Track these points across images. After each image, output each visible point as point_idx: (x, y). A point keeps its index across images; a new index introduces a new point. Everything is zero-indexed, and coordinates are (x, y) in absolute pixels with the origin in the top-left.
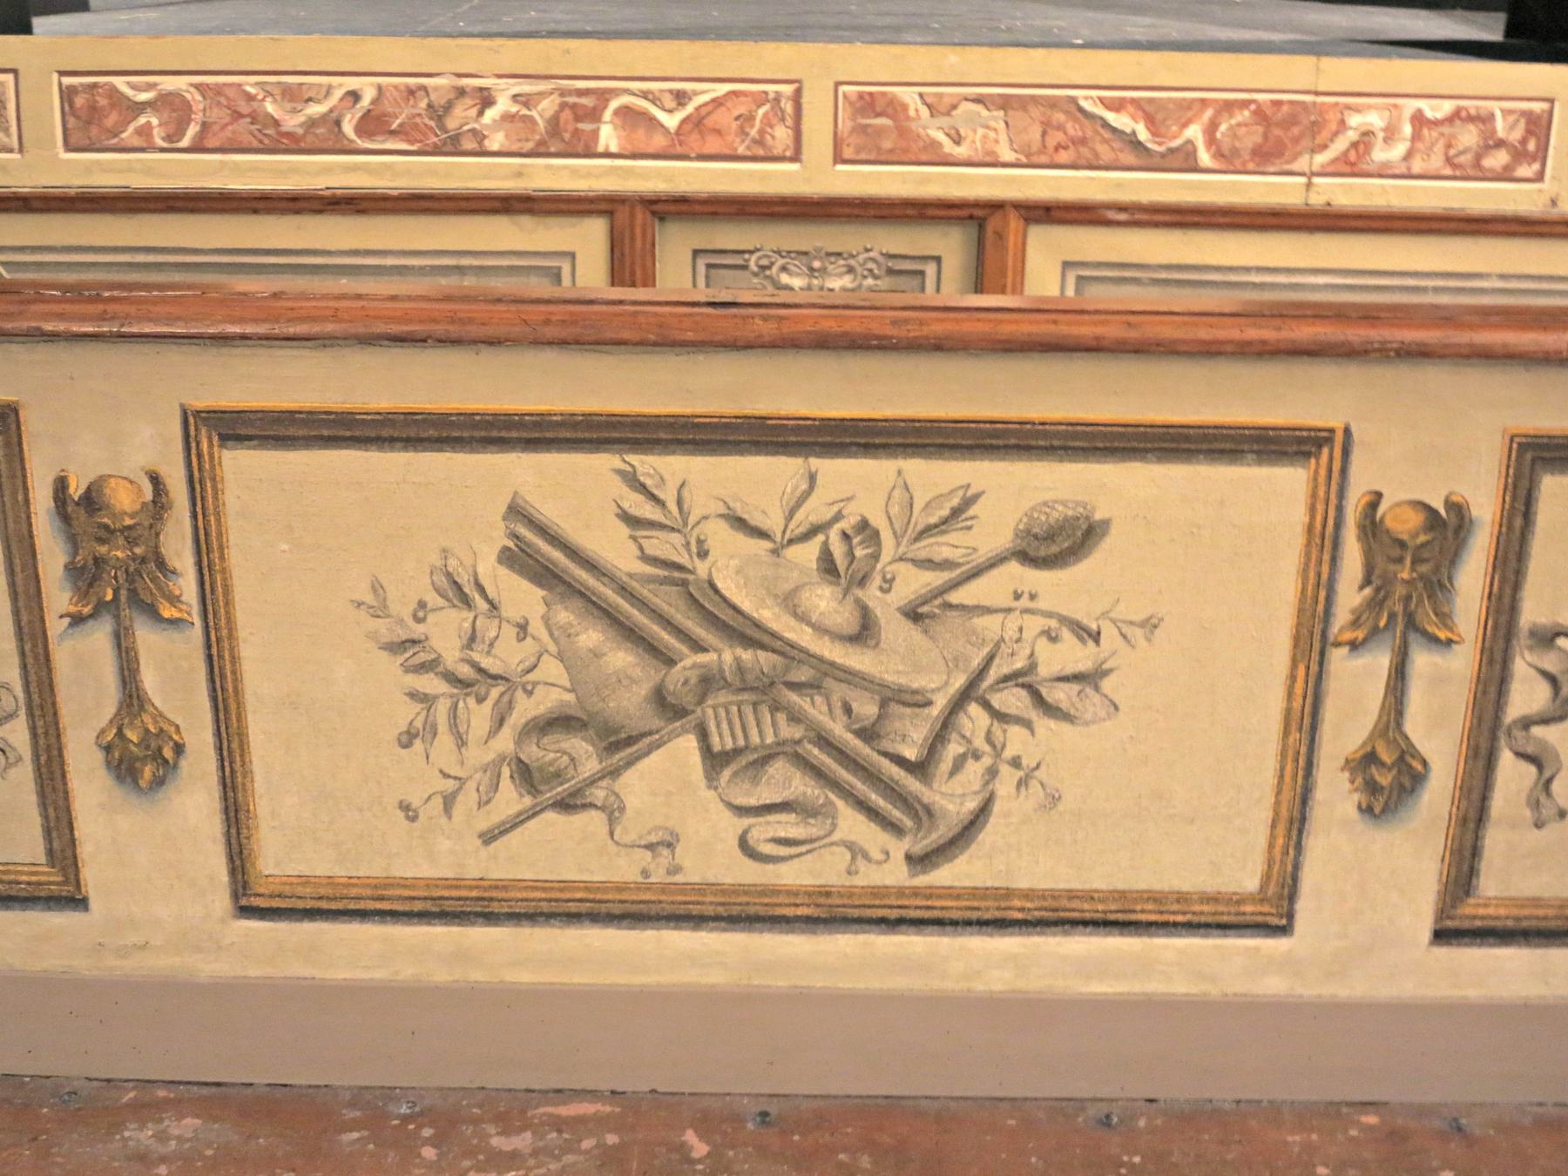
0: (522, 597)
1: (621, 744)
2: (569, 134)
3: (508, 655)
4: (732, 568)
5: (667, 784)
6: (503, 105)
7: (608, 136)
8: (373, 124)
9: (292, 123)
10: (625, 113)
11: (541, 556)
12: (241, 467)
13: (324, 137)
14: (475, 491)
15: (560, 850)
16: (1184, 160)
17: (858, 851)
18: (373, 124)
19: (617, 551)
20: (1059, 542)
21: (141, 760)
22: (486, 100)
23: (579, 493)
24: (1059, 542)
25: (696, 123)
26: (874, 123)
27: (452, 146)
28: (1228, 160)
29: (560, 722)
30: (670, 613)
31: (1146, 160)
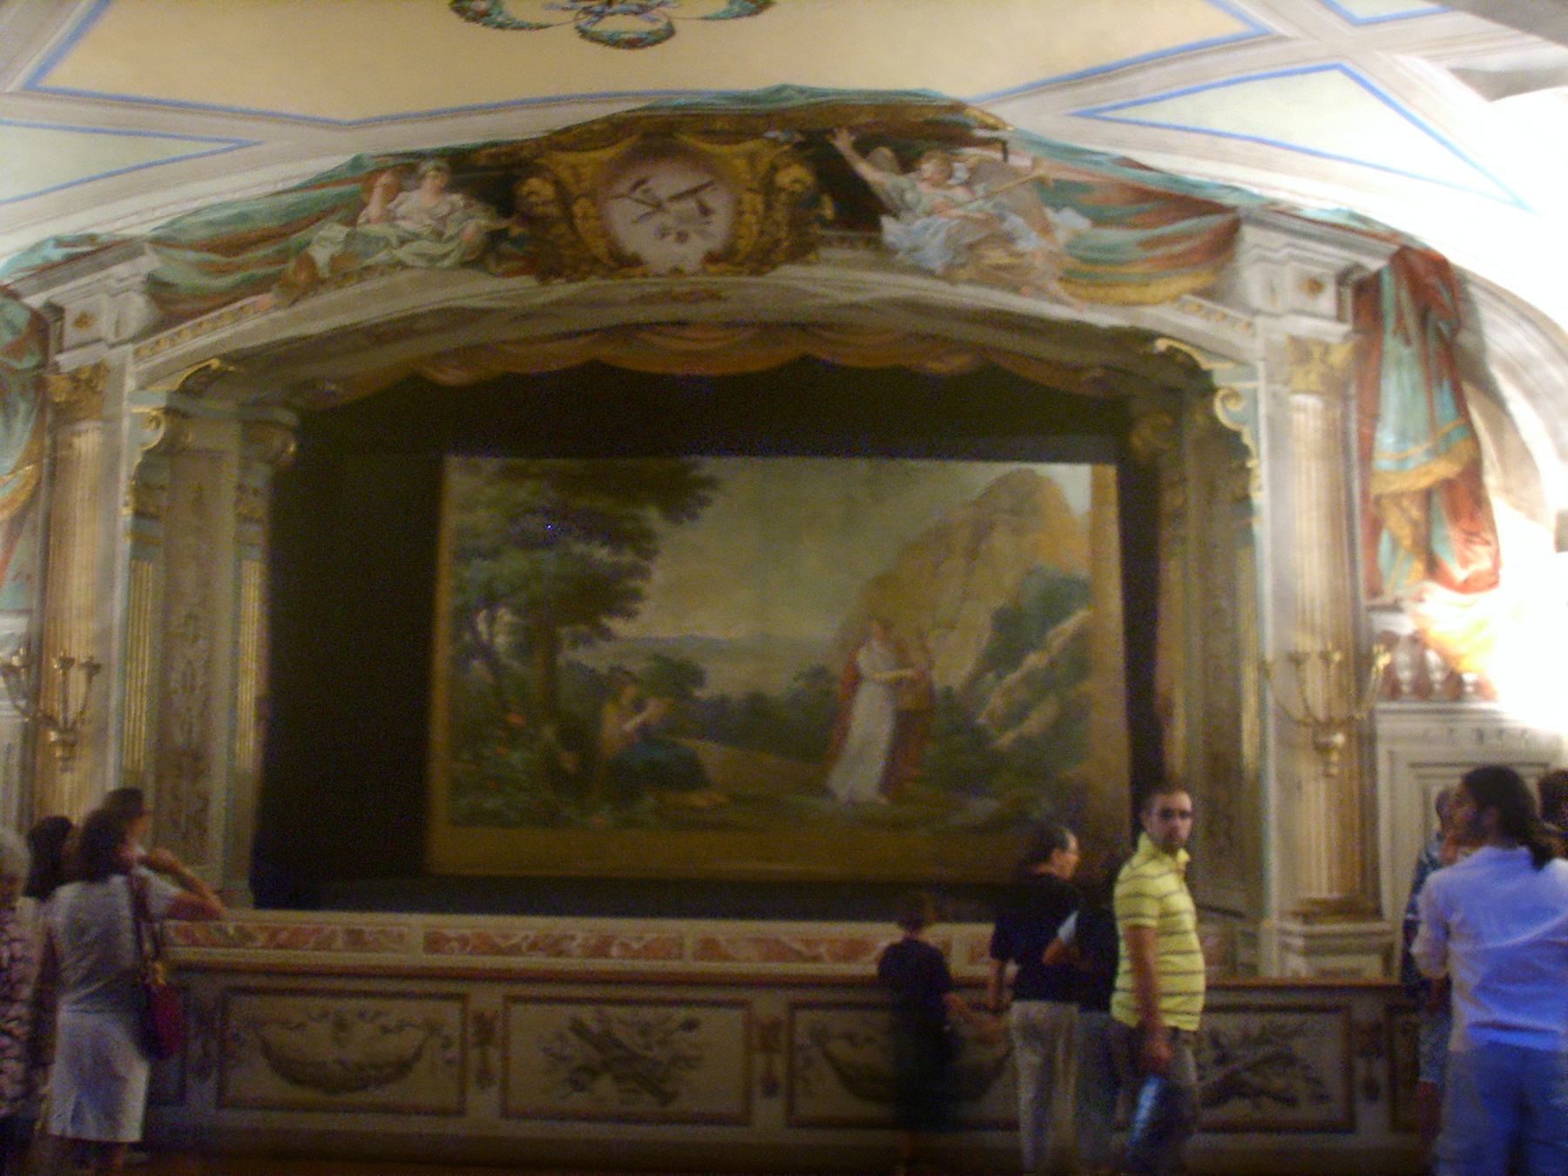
0: (573, 1039)
1: (594, 1073)
2: (601, 949)
3: (568, 1051)
4: (621, 1034)
5: (604, 1084)
6: (579, 941)
7: (615, 951)
8: (534, 946)
9: (503, 944)
10: (624, 946)
11: (578, 1028)
12: (518, 1010)
13: (514, 950)
14: (562, 1015)
15: (579, 1101)
16: (816, 959)
17: (646, 1103)
18: (534, 946)
19: (595, 1027)
20: (690, 1025)
21: (484, 1076)
22: (572, 938)
23: (587, 1014)
24: (690, 1025)
25: (646, 947)
26: (709, 948)
27: (560, 954)
28: (837, 958)
29: (578, 1070)
30: (603, 1041)
31: (800, 957)
